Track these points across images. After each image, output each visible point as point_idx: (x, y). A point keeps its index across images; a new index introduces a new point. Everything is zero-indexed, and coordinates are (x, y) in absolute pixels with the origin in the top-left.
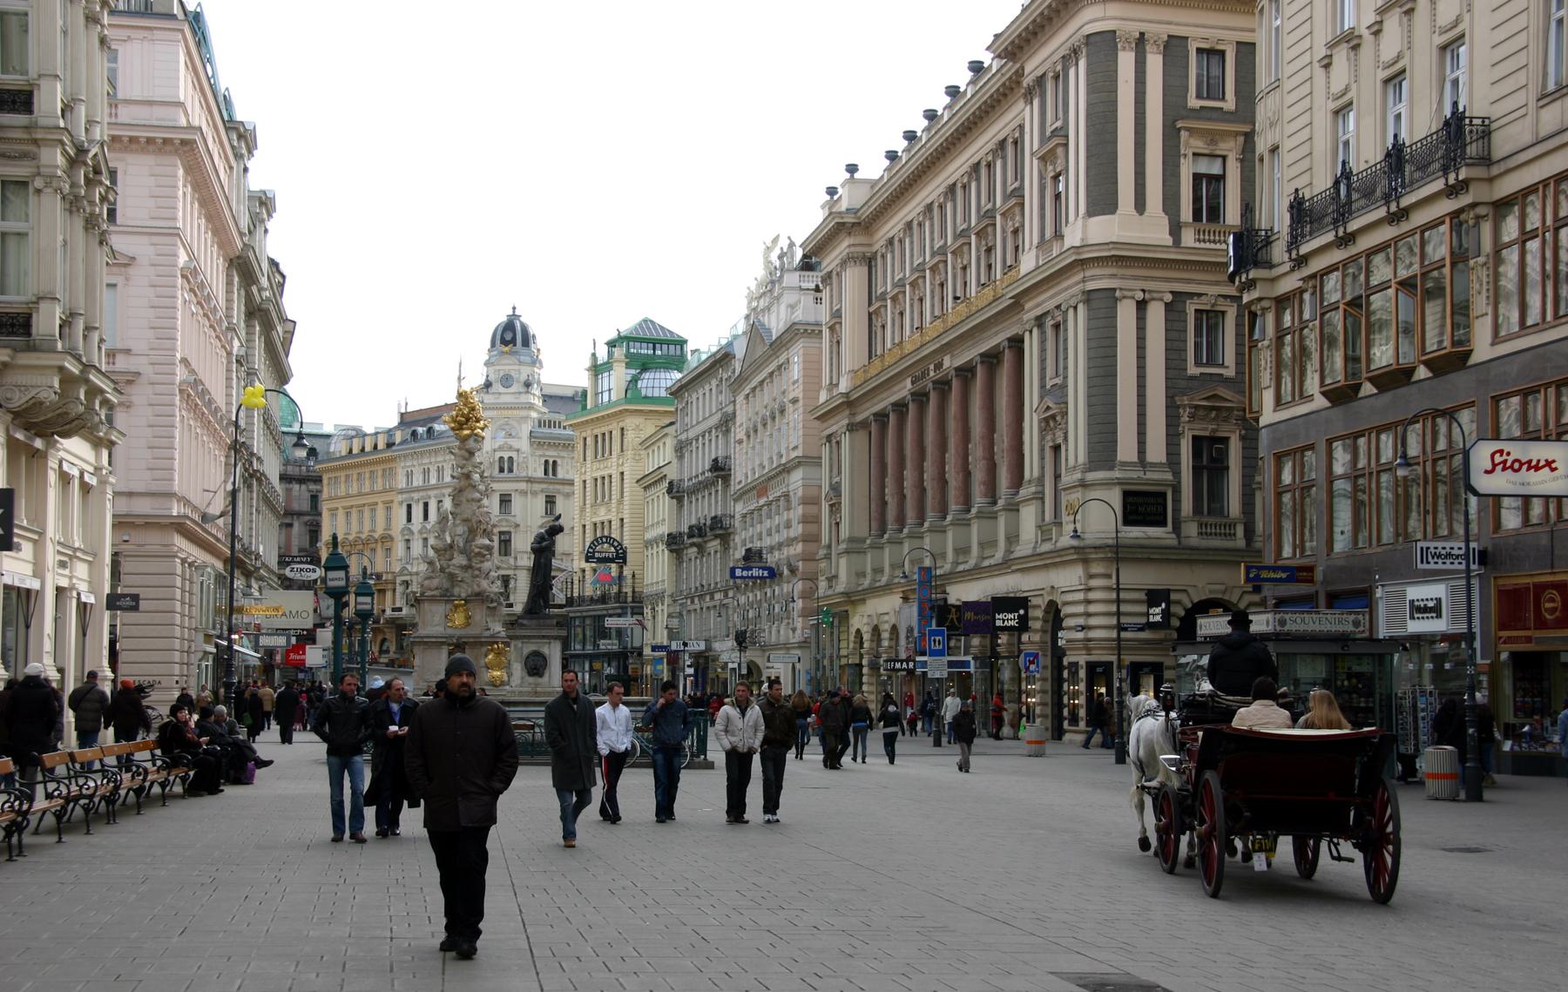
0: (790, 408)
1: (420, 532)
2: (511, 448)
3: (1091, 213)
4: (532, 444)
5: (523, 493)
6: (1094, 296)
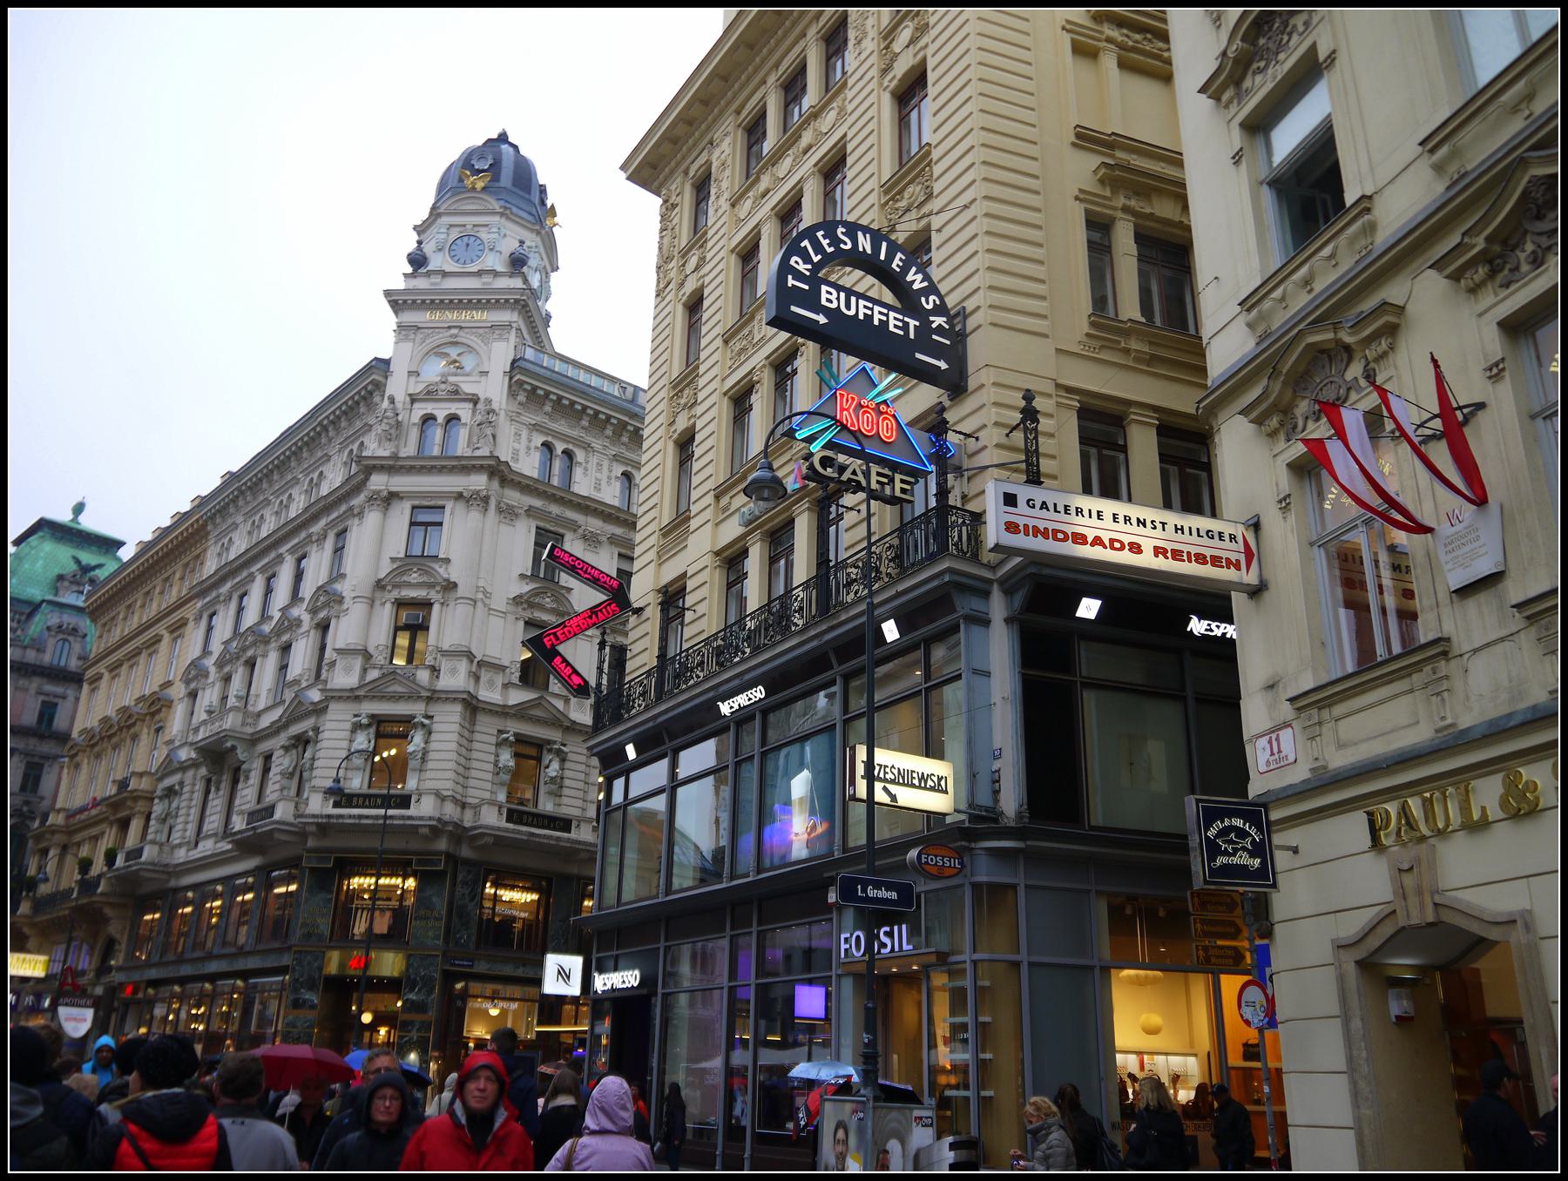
1: (220, 664)
2: (456, 395)
4: (514, 388)
5: (481, 500)
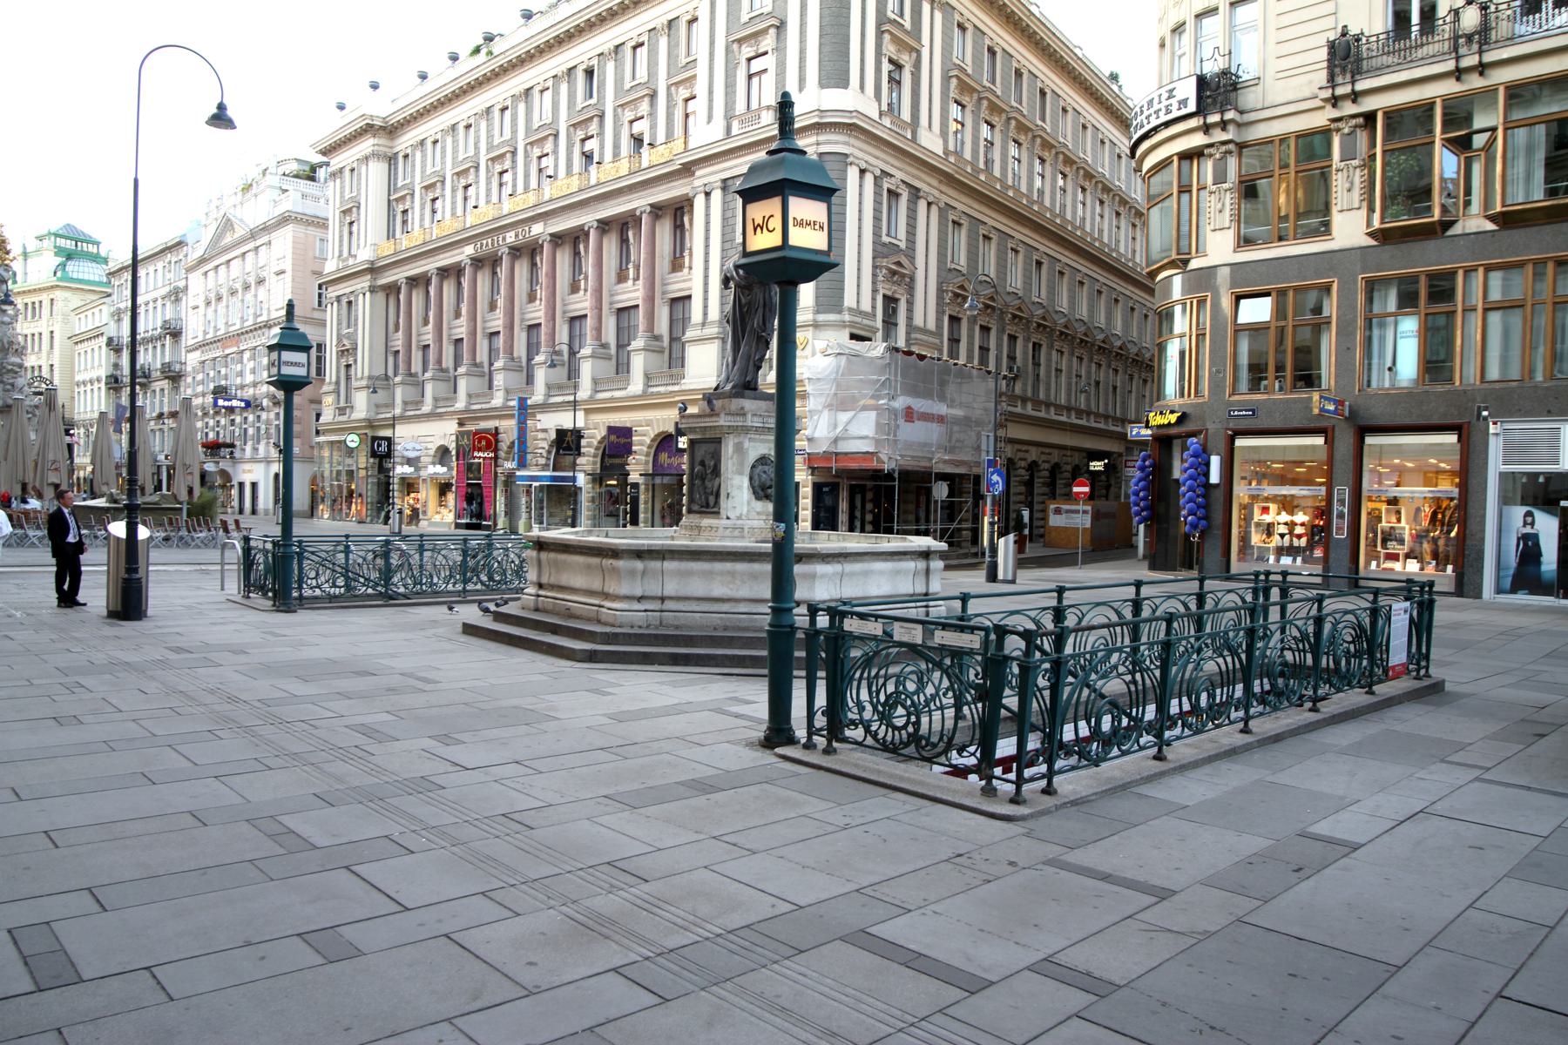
0: (272, 280)
3: (822, 85)
6: (827, 158)
